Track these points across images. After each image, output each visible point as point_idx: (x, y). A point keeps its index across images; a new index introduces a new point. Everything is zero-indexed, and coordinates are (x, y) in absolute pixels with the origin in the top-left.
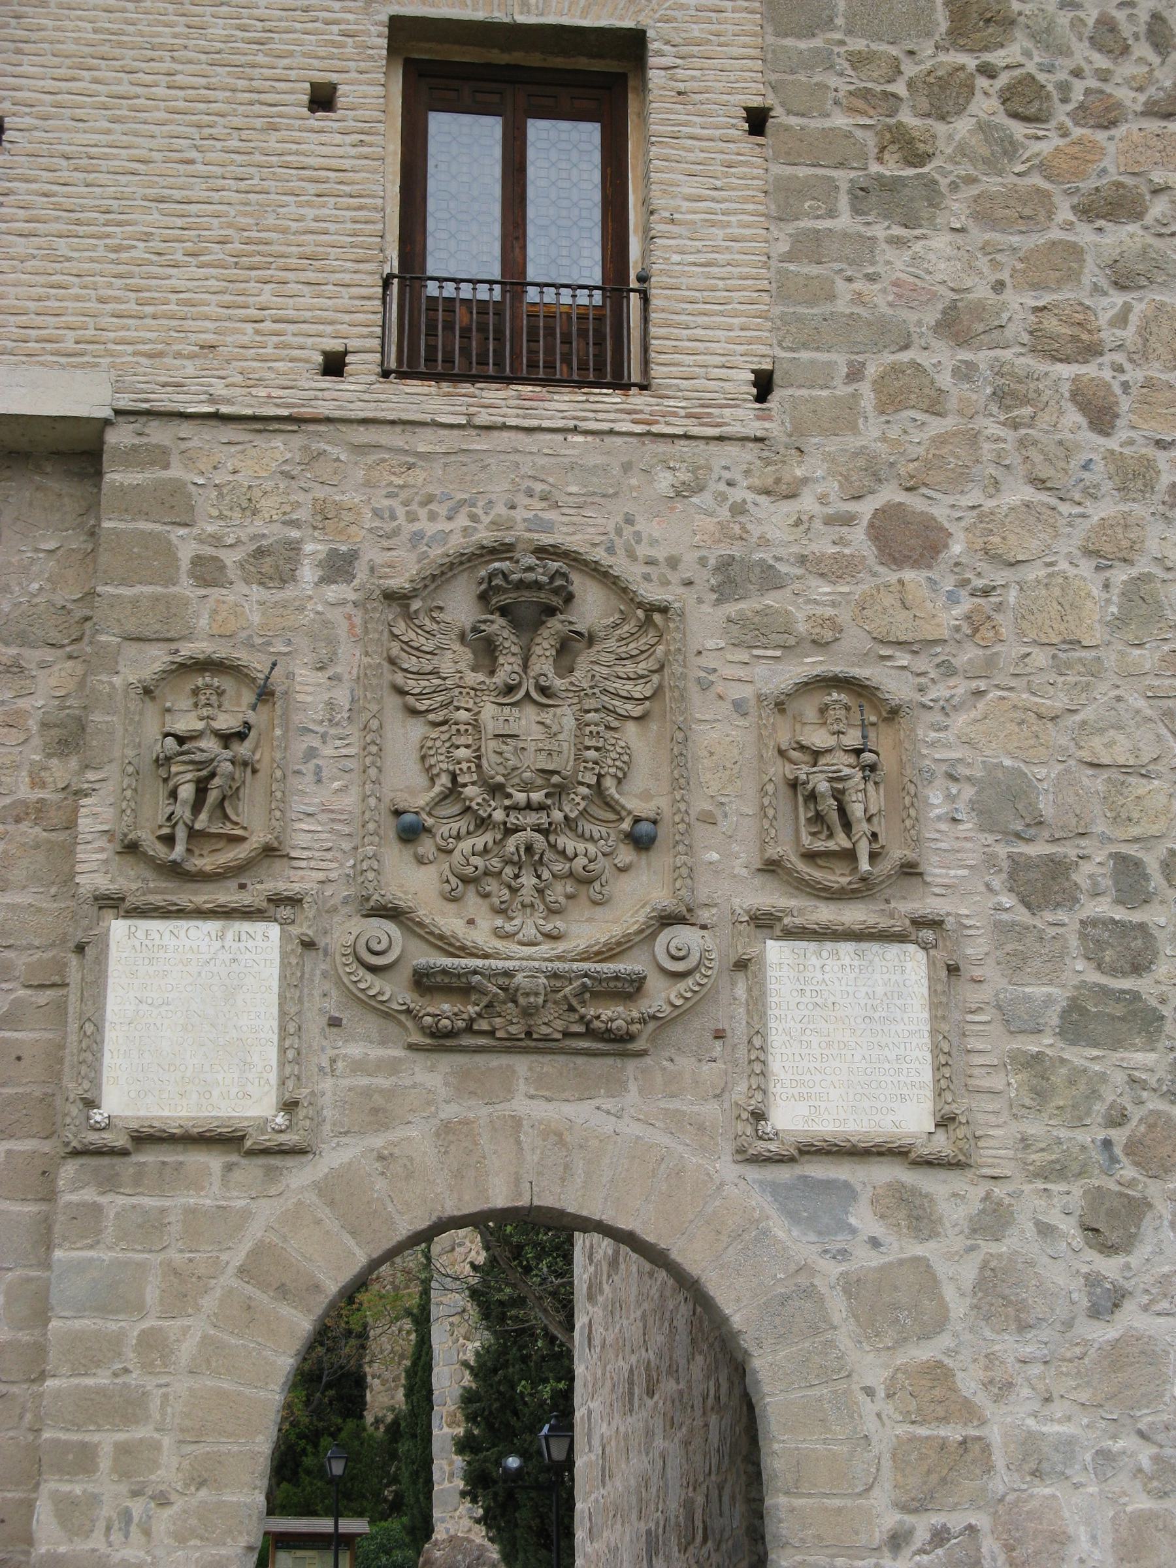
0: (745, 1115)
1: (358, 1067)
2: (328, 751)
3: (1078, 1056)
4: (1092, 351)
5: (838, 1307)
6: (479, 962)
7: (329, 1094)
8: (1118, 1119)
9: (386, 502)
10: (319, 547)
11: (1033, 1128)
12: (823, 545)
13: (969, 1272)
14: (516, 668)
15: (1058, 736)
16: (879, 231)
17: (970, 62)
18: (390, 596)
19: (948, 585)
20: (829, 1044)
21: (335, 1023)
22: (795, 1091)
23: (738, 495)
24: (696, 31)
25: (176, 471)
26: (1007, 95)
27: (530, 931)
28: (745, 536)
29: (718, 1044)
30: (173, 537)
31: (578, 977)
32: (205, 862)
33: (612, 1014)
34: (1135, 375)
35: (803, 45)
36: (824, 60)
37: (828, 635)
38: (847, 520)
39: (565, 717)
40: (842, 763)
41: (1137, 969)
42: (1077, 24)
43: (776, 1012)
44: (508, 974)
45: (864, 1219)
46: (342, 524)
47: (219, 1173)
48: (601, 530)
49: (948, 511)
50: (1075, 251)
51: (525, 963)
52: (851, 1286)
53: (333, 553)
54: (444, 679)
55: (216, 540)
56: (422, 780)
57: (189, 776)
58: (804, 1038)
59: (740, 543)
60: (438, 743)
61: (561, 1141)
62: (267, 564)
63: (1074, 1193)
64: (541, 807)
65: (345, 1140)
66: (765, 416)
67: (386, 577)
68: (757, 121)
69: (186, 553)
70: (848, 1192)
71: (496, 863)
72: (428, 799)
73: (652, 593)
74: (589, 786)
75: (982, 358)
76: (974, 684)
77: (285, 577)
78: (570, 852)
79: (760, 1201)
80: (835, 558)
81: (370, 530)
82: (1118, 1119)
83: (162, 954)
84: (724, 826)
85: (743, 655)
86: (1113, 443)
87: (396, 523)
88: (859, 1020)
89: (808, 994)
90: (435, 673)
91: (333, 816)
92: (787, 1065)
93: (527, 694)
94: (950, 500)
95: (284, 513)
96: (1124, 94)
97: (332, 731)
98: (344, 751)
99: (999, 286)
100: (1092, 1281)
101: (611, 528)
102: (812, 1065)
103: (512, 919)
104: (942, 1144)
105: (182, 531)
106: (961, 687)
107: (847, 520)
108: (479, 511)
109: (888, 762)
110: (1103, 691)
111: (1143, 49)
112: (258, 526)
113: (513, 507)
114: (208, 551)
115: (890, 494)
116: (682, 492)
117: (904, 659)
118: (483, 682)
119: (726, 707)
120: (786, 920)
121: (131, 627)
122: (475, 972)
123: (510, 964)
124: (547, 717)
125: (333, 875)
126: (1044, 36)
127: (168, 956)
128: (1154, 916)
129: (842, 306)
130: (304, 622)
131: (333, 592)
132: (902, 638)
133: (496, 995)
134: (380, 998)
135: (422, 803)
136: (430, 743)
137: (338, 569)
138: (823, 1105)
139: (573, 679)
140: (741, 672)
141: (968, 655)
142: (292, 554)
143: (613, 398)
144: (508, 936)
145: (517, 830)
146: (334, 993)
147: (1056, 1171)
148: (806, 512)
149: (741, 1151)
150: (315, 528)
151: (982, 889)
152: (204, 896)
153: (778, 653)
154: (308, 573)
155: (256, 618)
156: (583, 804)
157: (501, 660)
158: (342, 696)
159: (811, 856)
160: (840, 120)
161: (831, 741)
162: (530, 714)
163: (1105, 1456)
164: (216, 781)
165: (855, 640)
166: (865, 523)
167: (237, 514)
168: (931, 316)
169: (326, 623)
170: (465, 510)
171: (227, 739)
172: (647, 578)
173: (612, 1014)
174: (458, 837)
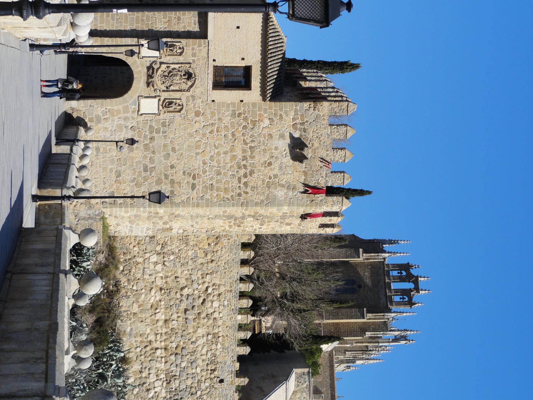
1: (146, 64)
3: (148, 126)
4: (217, 131)
5: (126, 104)
12: (197, 105)
13: (129, 116)
17: (249, 122)
23: (202, 97)
24: (251, 95)
25: (203, 46)
35: (251, 106)
36: (249, 107)
38: (199, 108)
41: (156, 132)
42: (254, 133)
45: (133, 107)
52: (127, 106)
66: (210, 101)
68: (242, 101)
75: (217, 122)
77: (193, 56)
79: (134, 98)
82: (142, 129)
86: (208, 133)
96: (246, 137)
99: (224, 124)
100: (128, 126)
111: (251, 139)
128: (161, 134)
143: (211, 86)
163: (113, 127)
168: (221, 117)
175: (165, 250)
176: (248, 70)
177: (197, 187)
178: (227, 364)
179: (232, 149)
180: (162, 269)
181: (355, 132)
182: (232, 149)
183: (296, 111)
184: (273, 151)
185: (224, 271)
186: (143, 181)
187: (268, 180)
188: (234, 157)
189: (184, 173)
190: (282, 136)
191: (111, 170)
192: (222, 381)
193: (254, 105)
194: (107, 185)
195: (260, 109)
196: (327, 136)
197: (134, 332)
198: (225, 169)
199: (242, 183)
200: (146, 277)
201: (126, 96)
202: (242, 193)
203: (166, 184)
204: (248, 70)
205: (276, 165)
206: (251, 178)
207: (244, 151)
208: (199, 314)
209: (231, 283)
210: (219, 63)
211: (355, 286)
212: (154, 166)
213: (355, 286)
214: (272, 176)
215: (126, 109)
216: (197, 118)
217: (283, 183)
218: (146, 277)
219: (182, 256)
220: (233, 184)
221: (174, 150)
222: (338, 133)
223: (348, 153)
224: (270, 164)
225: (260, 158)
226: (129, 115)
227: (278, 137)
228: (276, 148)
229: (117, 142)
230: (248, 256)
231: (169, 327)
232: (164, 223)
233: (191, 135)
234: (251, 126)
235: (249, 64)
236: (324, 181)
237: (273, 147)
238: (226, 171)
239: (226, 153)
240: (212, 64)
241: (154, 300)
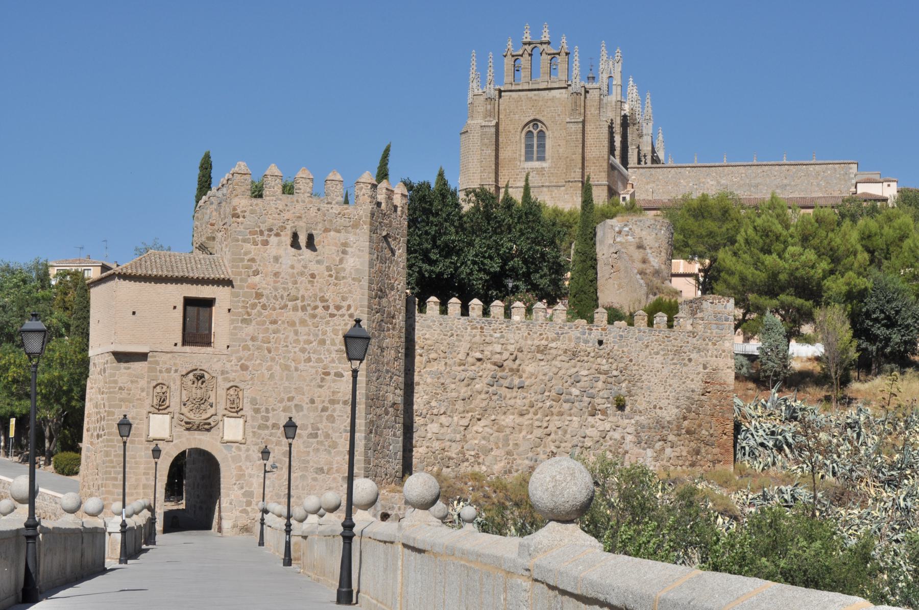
3: (259, 431)
4: (269, 342)
8: (263, 439)
11: (254, 439)
13: (245, 455)
15: (260, 393)
16: (244, 326)
18: (183, 376)
25: (157, 359)
26: (262, 306)
32: (160, 408)
33: (206, 427)
34: (274, 346)
40: (234, 397)
41: (267, 421)
45: (234, 449)
50: (268, 329)
52: (231, 457)
63: (258, 447)
68: (229, 310)
69: (158, 369)
70: (232, 447)
73: (214, 375)
77: (170, 372)
82: (263, 439)
104: (243, 441)
106: (248, 387)
109: (241, 396)
110: (266, 388)
111: (280, 299)
115: (243, 361)
116: (217, 361)
126: (267, 297)
128: (270, 415)
129: (239, 337)
141: (250, 383)
147: (256, 445)
152: (161, 412)
154: (172, 372)
160: (240, 310)
165: (237, 380)
171: (163, 393)
173: (206, 427)
175: (424, 412)
176: (189, 302)
177: (340, 370)
178: (579, 335)
179: (292, 324)
180: (449, 416)
181: (273, 165)
182: (292, 324)
183: (244, 241)
184: (295, 271)
185: (455, 336)
186: (330, 440)
187: (333, 278)
188: (303, 322)
189: (321, 387)
190: (276, 259)
191: (315, 479)
192: (600, 343)
193: (236, 295)
194: (334, 485)
195: (241, 287)
196: (279, 202)
197: (530, 455)
198: (317, 335)
199: (335, 312)
200: (458, 437)
201: (219, 458)
202: (349, 312)
203: (334, 410)
204: (189, 302)
205: (314, 268)
206: (330, 301)
207: (295, 309)
208: (511, 370)
209: (472, 329)
210: (179, 341)
211: (535, 132)
212: (310, 426)
213: (535, 132)
214: (327, 273)
215: (236, 459)
217: (338, 259)
218: (458, 437)
219: (434, 391)
220: (338, 324)
221: (290, 399)
222: (273, 188)
223: (300, 174)
224: (313, 276)
225: (304, 289)
226: (243, 456)
227: (278, 265)
228: (292, 267)
229: (265, 472)
230: (436, 305)
231: (527, 410)
232: (387, 413)
233: (272, 377)
234: (263, 300)
235: (182, 300)
236: (337, 206)
237: (290, 271)
238: (320, 332)
239: (296, 333)
240: (180, 348)
241: (492, 428)
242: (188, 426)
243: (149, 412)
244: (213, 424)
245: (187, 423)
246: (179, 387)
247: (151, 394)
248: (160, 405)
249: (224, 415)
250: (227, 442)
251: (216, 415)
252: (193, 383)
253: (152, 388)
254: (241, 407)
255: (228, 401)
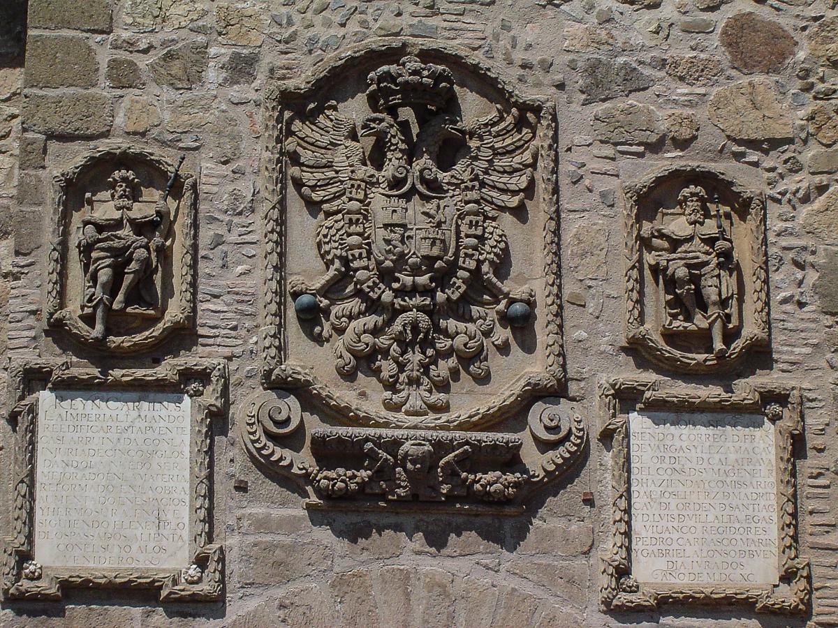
0: (611, 570)
1: (262, 525)
2: (233, 237)
6: (370, 432)
7: (236, 549)
9: (284, 10)
10: (223, 51)
14: (403, 162)
19: (795, 87)
20: (686, 505)
21: (242, 487)
22: (655, 548)
27: (415, 402)
28: (611, 41)
29: (587, 508)
30: (91, 43)
31: (461, 445)
33: (493, 480)
37: (686, 133)
38: (705, 29)
39: (450, 205)
40: (697, 250)
43: (639, 477)
44: (397, 443)
46: (244, 30)
47: (140, 619)
48: (480, 35)
49: (793, 21)
51: (412, 432)
53: (236, 57)
54: (337, 172)
55: (130, 45)
56: (320, 264)
57: (108, 261)
58: (663, 500)
59: (606, 47)
60: (333, 231)
61: (444, 593)
62: (176, 68)
64: (427, 292)
65: (250, 591)
67: (284, 78)
69: (104, 57)
71: (383, 341)
72: (323, 282)
73: (528, 94)
74: (468, 270)
76: (817, 179)
77: (192, 78)
78: (451, 330)
80: (692, 62)
81: (269, 36)
83: (85, 422)
84: (591, 306)
85: (609, 151)
87: (293, 29)
88: (713, 484)
89: (667, 460)
90: (329, 166)
91: (237, 297)
92: (648, 524)
93: (413, 188)
94: (796, 10)
95: (192, 20)
97: (236, 220)
98: (248, 238)
101: (489, 32)
102: (670, 525)
103: (400, 391)
105: (99, 38)
107: (705, 29)
108: (370, 18)
112: (167, 33)
113: (399, 14)
114: (122, 55)
117: (753, 156)
118: (372, 176)
119: (595, 197)
120: (647, 394)
121: (56, 125)
122: (367, 440)
123: (398, 433)
124: (430, 207)
125: (238, 351)
127: (90, 424)
130: (211, 118)
131: (235, 92)
132: (753, 136)
133: (386, 460)
134: (283, 463)
135: (318, 286)
136: (325, 231)
137: (240, 71)
138: (680, 561)
139: (453, 172)
140: (608, 166)
142: (198, 57)
144: (396, 408)
145: (405, 309)
146: (239, 458)
148: (666, 20)
149: (607, 603)
150: (220, 34)
151: (825, 364)
153: (641, 149)
154: (213, 75)
155: (167, 116)
156: (464, 287)
157: (389, 155)
158: (245, 188)
159: (671, 337)
161: (688, 230)
162: (416, 205)
164: (133, 266)
166: (719, 30)
167: (148, 21)
169: (232, 121)
170: (357, 17)
171: (142, 228)
172: (521, 79)
173: (493, 480)
174: (351, 317)
216: (801, 55)
242: (339, 477)
243: (34, 378)
244: (537, 463)
245: (328, 452)
246: (264, 184)
247: (49, 237)
248: (116, 322)
249: (626, 398)
250: (669, 604)
251: (556, 392)
252: (377, 158)
253: (53, 197)
254: (751, 329)
255: (656, 297)
